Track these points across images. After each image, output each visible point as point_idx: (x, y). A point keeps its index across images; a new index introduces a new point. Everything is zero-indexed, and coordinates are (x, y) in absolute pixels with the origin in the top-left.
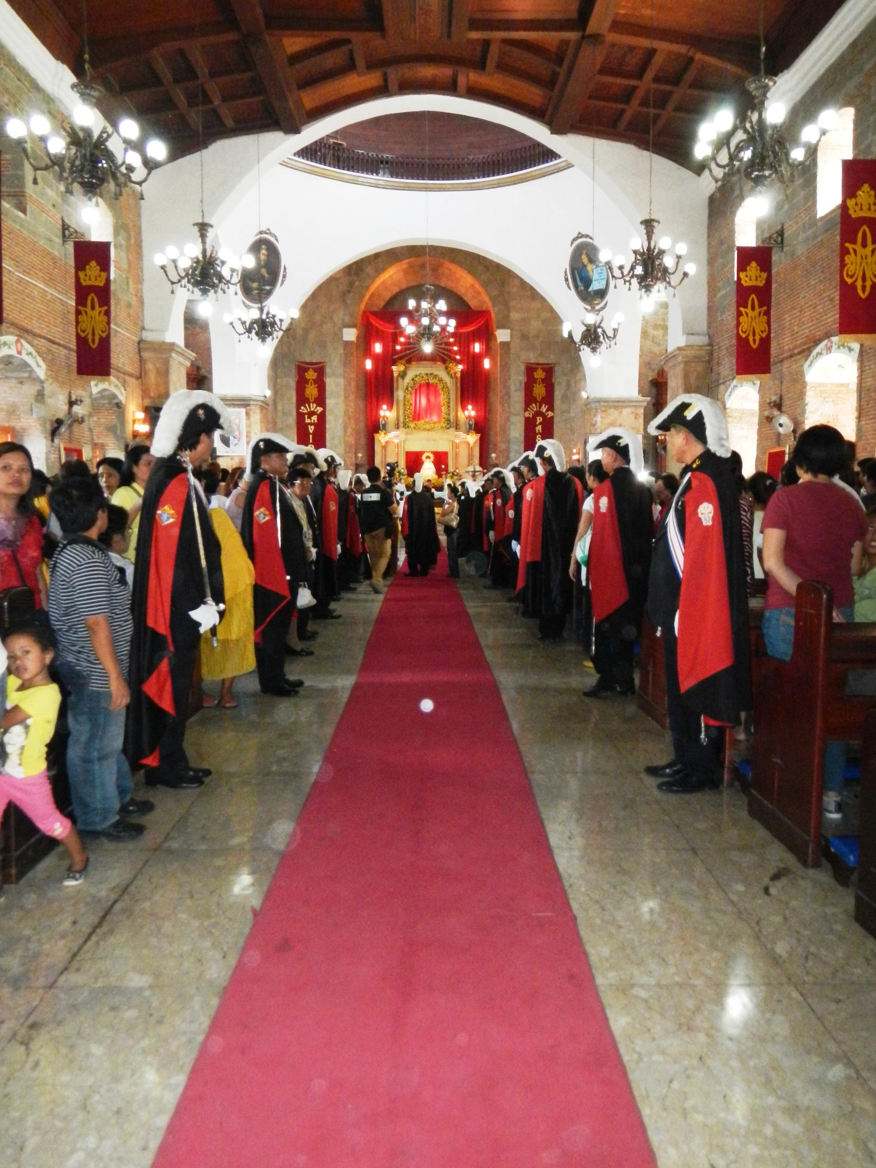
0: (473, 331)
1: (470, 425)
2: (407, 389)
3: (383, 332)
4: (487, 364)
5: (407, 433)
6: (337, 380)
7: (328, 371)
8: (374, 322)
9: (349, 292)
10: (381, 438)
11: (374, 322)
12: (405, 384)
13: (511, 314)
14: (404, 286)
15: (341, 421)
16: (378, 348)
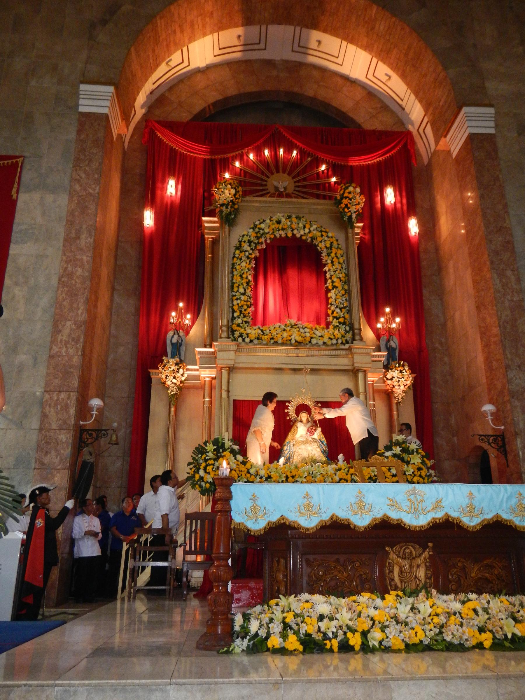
0: (379, 163)
1: (390, 350)
2: (239, 247)
3: (182, 154)
4: (413, 227)
5: (238, 350)
6: (50, 198)
7: (27, 175)
8: (167, 139)
9: (104, 22)
10: (170, 375)
11: (167, 139)
12: (234, 242)
13: (488, 85)
14: (232, 91)
15: (45, 301)
16: (171, 188)
